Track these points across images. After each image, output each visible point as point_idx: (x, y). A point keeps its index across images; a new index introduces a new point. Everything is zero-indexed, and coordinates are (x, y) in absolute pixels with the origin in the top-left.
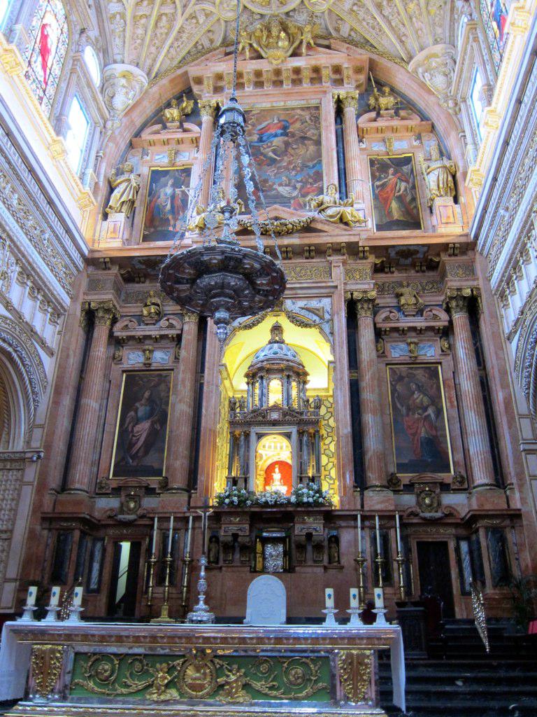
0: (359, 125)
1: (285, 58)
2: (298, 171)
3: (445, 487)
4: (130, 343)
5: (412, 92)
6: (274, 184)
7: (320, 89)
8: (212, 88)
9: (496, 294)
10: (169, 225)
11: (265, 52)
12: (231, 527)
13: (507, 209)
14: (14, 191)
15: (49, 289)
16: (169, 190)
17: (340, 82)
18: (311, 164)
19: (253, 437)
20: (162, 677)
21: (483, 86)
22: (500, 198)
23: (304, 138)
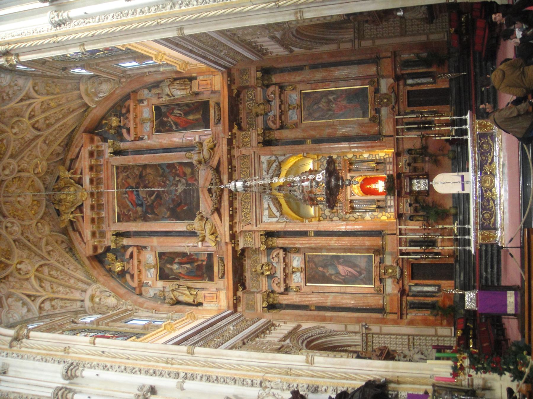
0: (132, 139)
1: (83, 189)
2: (166, 180)
3: (377, 91)
4: (287, 282)
5: (110, 104)
6: (175, 195)
7: (106, 165)
8: (101, 240)
9: (263, 58)
10: (202, 264)
11: (78, 203)
12: (405, 208)
13: (221, 51)
14: (212, 340)
15: (262, 327)
16: (175, 266)
17: (100, 153)
18: (161, 171)
19: (353, 198)
20: (489, 194)
21: (135, 61)
22: (214, 54)
23: (141, 176)
